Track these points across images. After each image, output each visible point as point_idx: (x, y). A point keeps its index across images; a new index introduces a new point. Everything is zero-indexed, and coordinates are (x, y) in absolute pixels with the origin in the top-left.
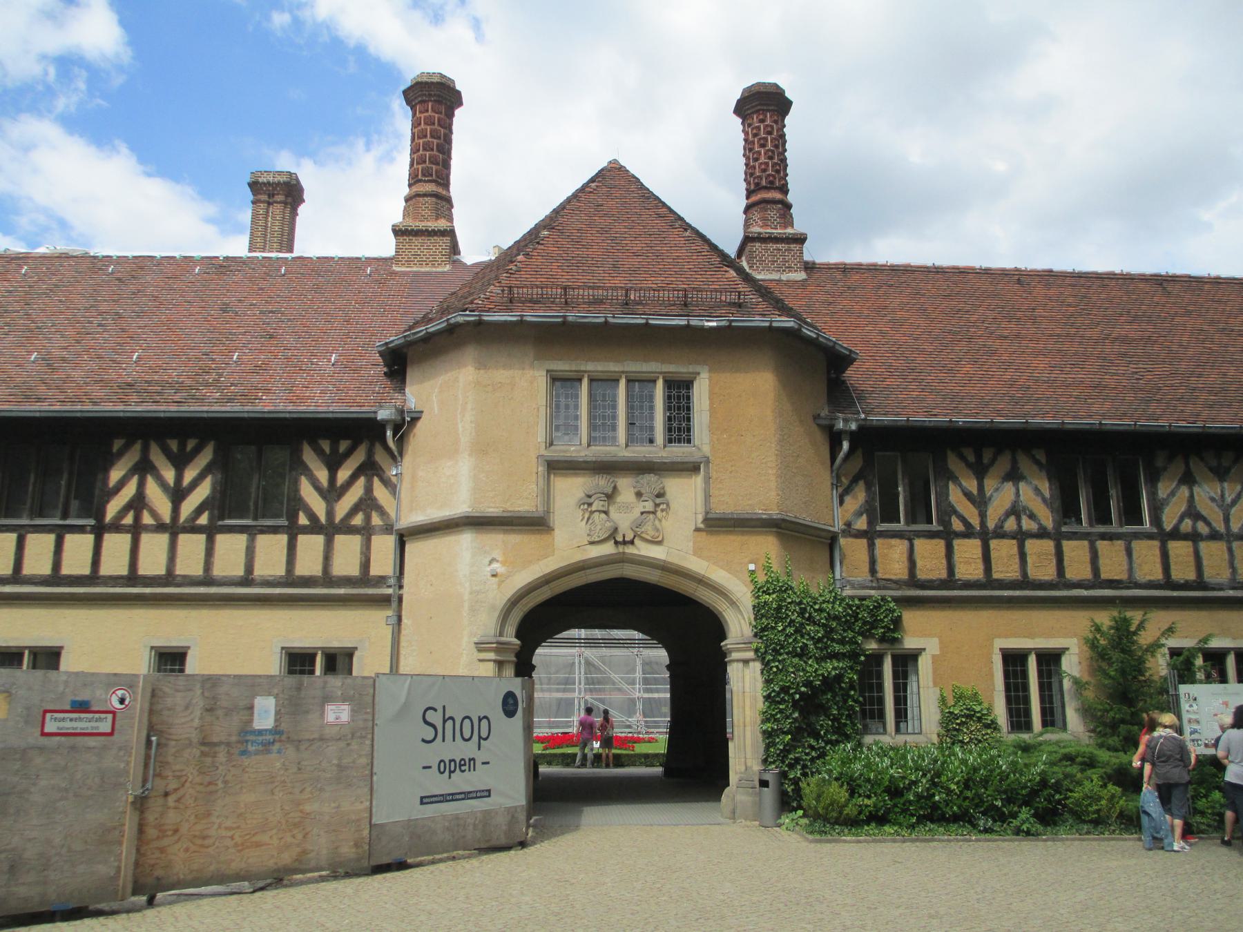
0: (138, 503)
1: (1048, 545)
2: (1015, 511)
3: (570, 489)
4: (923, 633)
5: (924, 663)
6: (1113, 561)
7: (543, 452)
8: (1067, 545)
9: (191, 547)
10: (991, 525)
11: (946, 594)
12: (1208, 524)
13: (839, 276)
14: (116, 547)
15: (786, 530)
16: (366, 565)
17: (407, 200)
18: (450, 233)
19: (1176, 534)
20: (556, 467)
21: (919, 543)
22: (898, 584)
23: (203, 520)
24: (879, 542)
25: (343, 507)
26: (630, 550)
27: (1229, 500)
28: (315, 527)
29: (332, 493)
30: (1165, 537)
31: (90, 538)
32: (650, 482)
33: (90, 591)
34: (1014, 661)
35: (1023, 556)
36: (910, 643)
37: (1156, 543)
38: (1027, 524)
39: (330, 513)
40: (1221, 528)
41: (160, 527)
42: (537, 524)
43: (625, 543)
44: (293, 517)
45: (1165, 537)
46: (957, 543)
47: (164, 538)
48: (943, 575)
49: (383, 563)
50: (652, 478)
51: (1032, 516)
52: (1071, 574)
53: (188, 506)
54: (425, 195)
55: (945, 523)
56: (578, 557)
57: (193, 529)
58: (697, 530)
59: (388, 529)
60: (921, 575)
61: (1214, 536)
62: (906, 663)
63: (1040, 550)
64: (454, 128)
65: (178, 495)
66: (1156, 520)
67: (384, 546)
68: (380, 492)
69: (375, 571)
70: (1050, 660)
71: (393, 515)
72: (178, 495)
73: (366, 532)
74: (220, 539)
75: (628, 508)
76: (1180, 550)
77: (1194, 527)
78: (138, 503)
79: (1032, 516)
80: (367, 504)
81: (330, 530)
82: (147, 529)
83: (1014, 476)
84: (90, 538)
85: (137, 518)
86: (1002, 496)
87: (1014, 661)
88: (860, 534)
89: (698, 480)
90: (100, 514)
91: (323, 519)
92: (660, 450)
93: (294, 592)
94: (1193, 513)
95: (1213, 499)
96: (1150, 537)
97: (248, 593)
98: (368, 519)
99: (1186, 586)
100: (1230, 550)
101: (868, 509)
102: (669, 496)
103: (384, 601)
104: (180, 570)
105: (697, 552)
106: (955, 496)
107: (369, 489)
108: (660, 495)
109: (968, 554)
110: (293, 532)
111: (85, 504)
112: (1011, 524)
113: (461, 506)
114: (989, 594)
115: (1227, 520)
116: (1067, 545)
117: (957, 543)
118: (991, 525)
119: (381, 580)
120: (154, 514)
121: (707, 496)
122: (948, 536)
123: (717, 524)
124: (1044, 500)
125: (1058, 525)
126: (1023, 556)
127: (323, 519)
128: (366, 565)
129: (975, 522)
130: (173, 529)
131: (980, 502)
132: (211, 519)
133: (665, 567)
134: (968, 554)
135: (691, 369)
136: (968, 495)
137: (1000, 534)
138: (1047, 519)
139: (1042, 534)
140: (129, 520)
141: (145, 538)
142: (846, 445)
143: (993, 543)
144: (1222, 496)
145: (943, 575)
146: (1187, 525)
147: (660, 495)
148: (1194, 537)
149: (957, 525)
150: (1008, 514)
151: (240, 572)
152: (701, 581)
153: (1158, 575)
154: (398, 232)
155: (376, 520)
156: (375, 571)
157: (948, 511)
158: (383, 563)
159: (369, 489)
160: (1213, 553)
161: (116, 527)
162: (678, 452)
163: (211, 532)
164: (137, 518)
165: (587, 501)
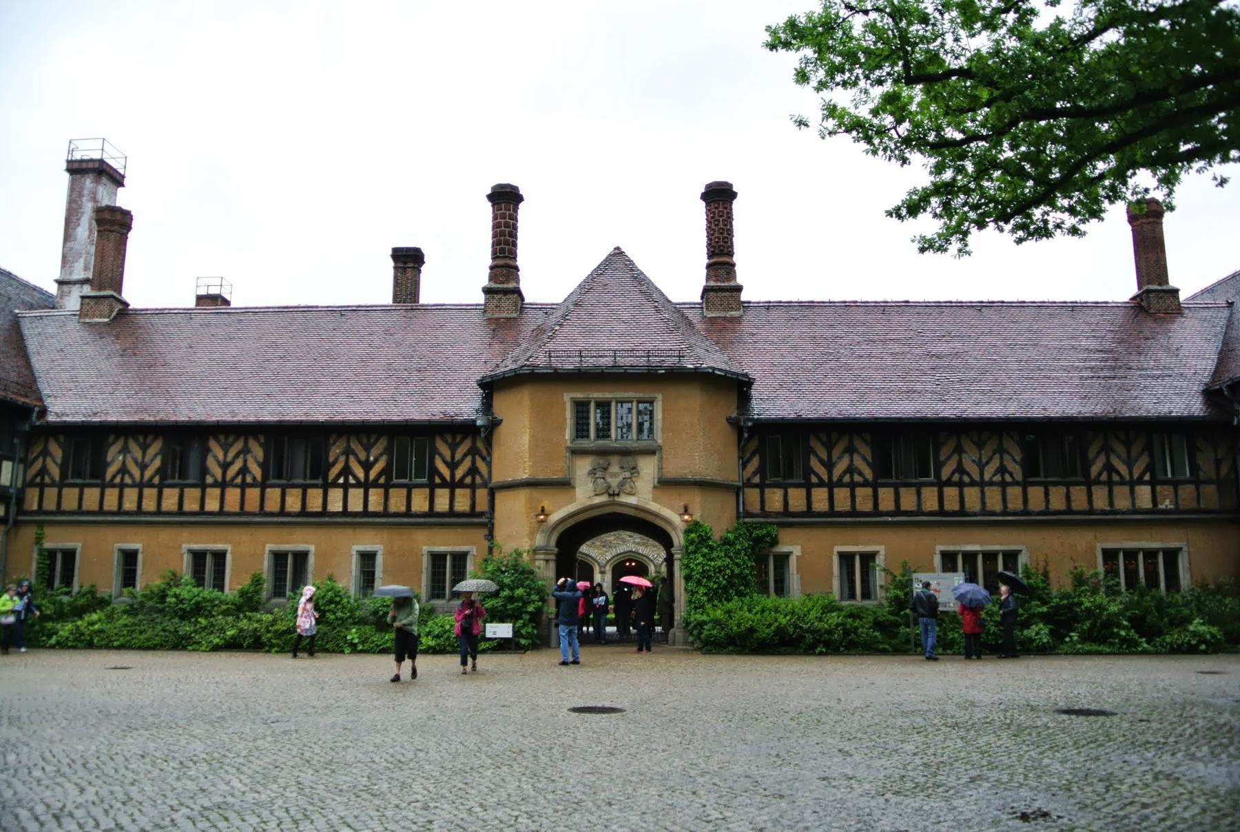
0: (346, 471)
1: (869, 491)
2: (851, 470)
3: (583, 466)
5: (793, 561)
6: (908, 500)
7: (569, 444)
8: (881, 491)
9: (375, 497)
10: (835, 479)
11: (808, 519)
12: (969, 475)
13: (764, 311)
14: (336, 496)
16: (473, 505)
17: (492, 268)
18: (518, 292)
19: (949, 483)
20: (576, 452)
21: (791, 491)
22: (778, 514)
23: (382, 481)
24: (767, 490)
25: (459, 473)
26: (616, 499)
27: (984, 461)
28: (444, 484)
29: (453, 466)
30: (941, 485)
31: (320, 491)
32: (629, 461)
33: (323, 519)
34: (846, 559)
35: (853, 497)
36: (782, 548)
37: (936, 489)
38: (857, 478)
39: (453, 476)
40: (976, 477)
41: (359, 485)
42: (565, 485)
43: (614, 495)
44: (431, 479)
45: (941, 485)
46: (813, 490)
47: (361, 491)
48: (804, 509)
49: (482, 505)
50: (630, 458)
51: (860, 474)
52: (882, 508)
53: (372, 475)
54: (502, 266)
55: (808, 479)
56: (589, 503)
57: (375, 485)
58: (655, 487)
59: (485, 485)
60: (791, 509)
61: (973, 483)
62: (783, 559)
63: (864, 494)
64: (519, 217)
65: (367, 466)
66: (938, 475)
67: (482, 494)
68: (480, 464)
69: (478, 509)
70: (868, 558)
71: (486, 475)
72: (367, 466)
73: (473, 487)
74: (391, 491)
75: (615, 475)
76: (951, 492)
77: (961, 478)
79: (860, 474)
80: (473, 471)
81: (452, 485)
82: (353, 486)
83: (850, 450)
84: (320, 491)
85: (346, 480)
87: (846, 559)
88: (755, 486)
89: (656, 458)
90: (326, 478)
91: (448, 478)
93: (432, 519)
94: (960, 469)
95: (973, 461)
96: (932, 484)
97: (408, 520)
98: (473, 479)
99: (954, 514)
100: (983, 493)
101: (761, 470)
102: (639, 468)
103: (483, 525)
104: (371, 508)
105: (655, 500)
106: (814, 463)
107: (474, 463)
108: (634, 468)
109: (820, 499)
110: (432, 487)
111: (318, 473)
112: (847, 479)
113: (524, 475)
114: (832, 519)
115: (982, 474)
116: (881, 491)
117: (813, 490)
118: (835, 479)
119: (482, 514)
120: (355, 477)
121: (660, 469)
122: (809, 487)
123: (665, 484)
124: (868, 464)
125: (875, 477)
126: (853, 497)
127: (448, 478)
128: (473, 505)
129: (825, 478)
130: (366, 485)
131: (829, 466)
132: (386, 480)
133: (637, 508)
134: (820, 499)
135: (652, 395)
136: (821, 461)
137: (840, 484)
138: (869, 474)
139: (865, 484)
140: (341, 481)
141: (351, 491)
142: (746, 435)
143: (836, 490)
144: (980, 459)
145: (804, 509)
146: (956, 477)
147: (634, 468)
148: (961, 485)
149: (814, 479)
150: (845, 473)
151: (403, 509)
152: (657, 515)
153: (936, 507)
154: (487, 291)
155: (478, 480)
156: (478, 509)
157: (809, 471)
158: (482, 505)
159: (474, 463)
160: (972, 494)
161: (335, 485)
162: (645, 443)
163: (387, 487)
164: (346, 480)
165: (592, 472)
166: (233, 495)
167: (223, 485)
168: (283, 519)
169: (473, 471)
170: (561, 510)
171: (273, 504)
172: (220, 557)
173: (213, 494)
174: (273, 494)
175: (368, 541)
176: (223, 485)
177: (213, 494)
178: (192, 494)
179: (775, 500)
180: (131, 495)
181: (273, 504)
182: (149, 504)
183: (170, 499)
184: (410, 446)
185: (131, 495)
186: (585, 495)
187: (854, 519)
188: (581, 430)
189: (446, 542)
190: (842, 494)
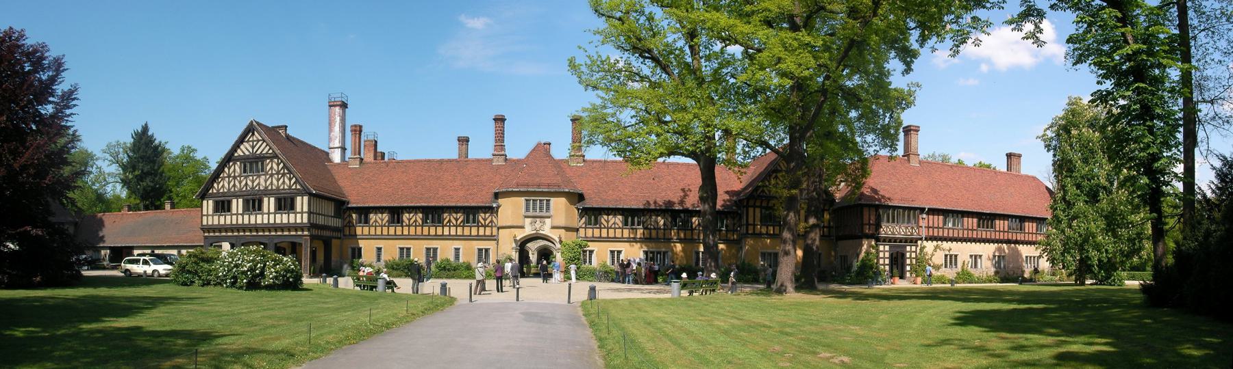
0: (450, 221)
3: (528, 221)
4: (592, 246)
9: (460, 229)
11: (600, 239)
14: (446, 229)
15: (568, 229)
33: (442, 237)
42: (522, 227)
65: (457, 220)
67: (495, 229)
72: (457, 220)
78: (450, 221)
80: (491, 221)
81: (485, 226)
86: (612, 219)
92: (544, 214)
93: (478, 238)
109: (604, 232)
111: (438, 221)
114: (608, 240)
131: (608, 222)
166: (412, 229)
167: (409, 226)
168: (429, 237)
169: (491, 221)
170: (520, 235)
171: (425, 232)
172: (409, 249)
173: (406, 229)
174: (426, 229)
175: (457, 244)
176: (409, 226)
177: (406, 229)
178: (399, 229)
179: (590, 233)
180: (379, 229)
181: (425, 232)
182: (385, 232)
183: (392, 230)
184: (470, 213)
185: (379, 229)
186: (528, 231)
187: (615, 240)
188: (527, 209)
189: (483, 245)
190: (611, 231)
